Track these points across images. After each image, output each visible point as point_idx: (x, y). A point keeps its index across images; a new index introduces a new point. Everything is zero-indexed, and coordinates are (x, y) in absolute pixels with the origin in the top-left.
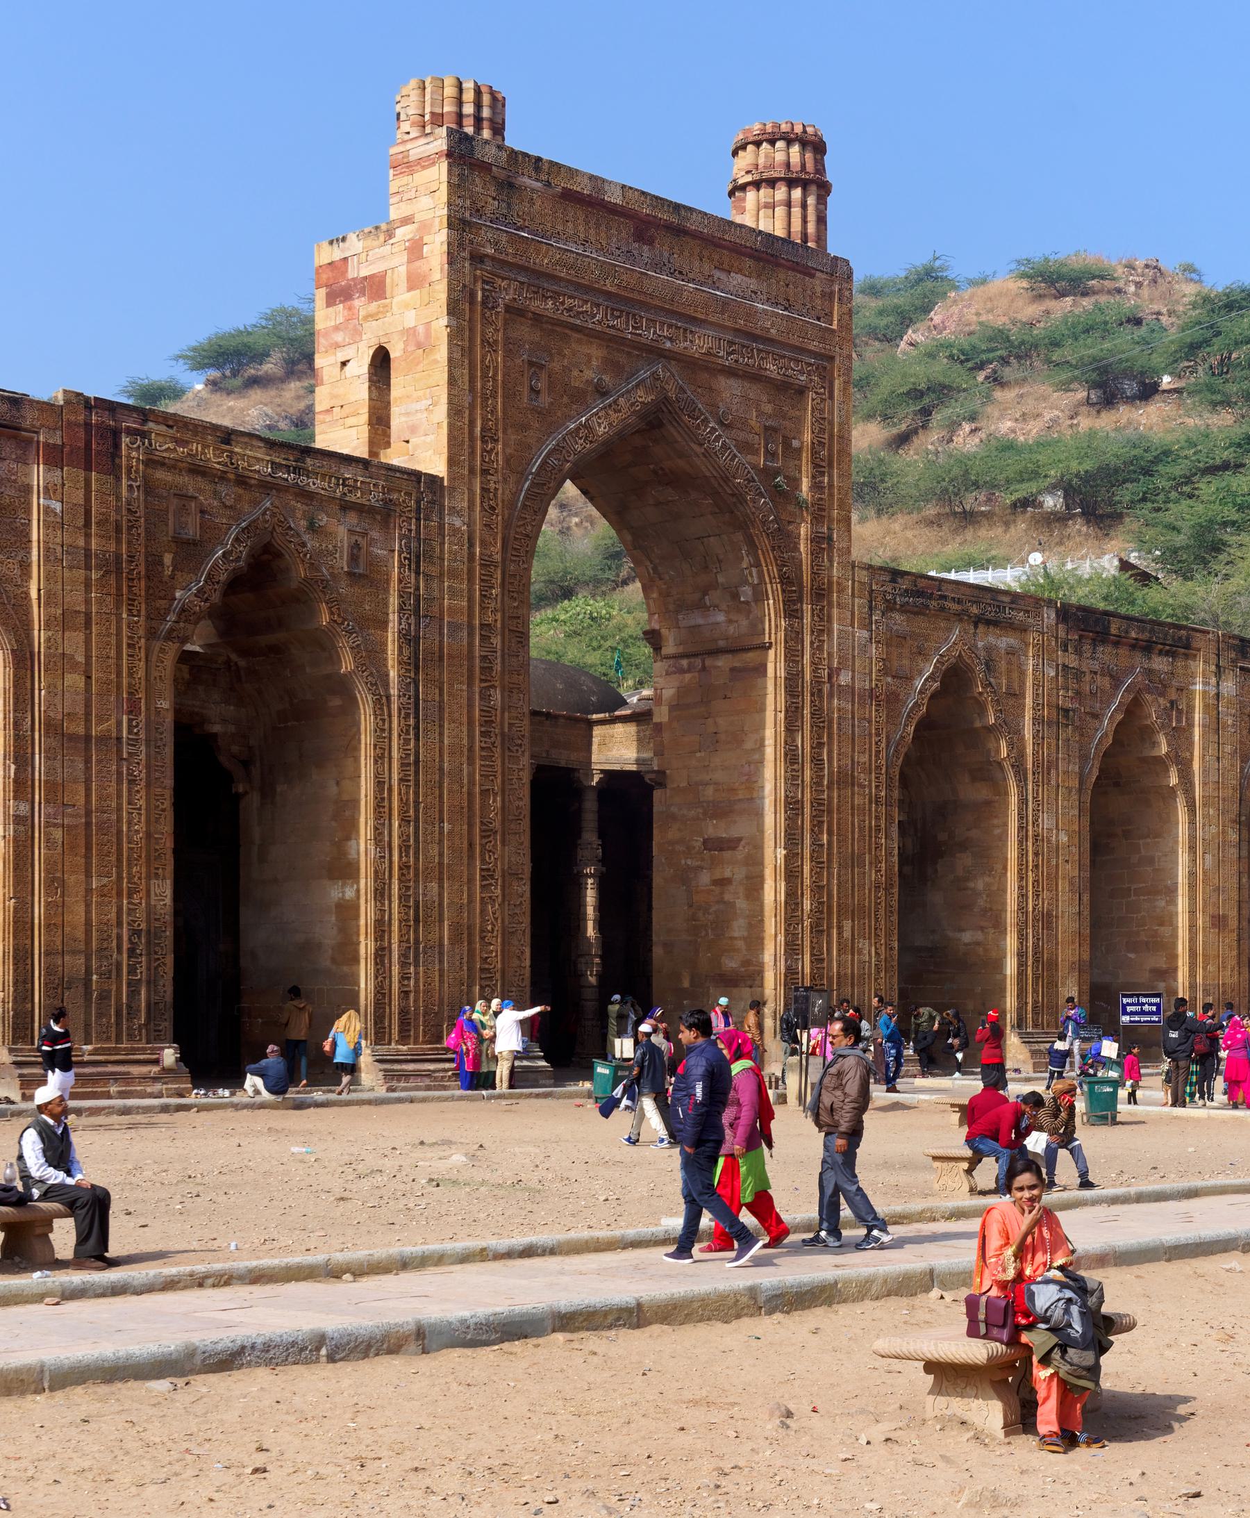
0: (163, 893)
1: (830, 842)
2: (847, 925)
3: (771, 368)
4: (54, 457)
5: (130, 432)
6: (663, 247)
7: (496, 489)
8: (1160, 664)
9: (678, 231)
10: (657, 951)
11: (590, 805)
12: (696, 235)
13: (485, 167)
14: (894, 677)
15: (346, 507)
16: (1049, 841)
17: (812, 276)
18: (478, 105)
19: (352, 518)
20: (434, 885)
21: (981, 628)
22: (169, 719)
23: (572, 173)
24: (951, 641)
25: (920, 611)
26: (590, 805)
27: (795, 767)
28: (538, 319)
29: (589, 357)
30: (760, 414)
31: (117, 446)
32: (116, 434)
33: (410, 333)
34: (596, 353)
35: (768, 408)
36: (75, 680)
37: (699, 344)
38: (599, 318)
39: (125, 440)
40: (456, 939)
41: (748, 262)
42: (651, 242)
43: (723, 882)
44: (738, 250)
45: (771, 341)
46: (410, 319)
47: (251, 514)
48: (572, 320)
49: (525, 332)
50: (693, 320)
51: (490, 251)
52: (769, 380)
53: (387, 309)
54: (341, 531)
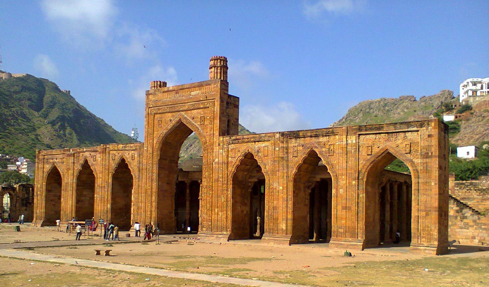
4: (100, 153)
13: (151, 94)
15: (132, 150)
16: (276, 189)
18: (157, 84)
21: (257, 143)
27: (206, 179)
28: (159, 113)
32: (106, 148)
34: (170, 114)
36: (101, 180)
37: (186, 108)
38: (168, 110)
41: (197, 88)
47: (120, 154)
51: (151, 106)
52: (202, 108)
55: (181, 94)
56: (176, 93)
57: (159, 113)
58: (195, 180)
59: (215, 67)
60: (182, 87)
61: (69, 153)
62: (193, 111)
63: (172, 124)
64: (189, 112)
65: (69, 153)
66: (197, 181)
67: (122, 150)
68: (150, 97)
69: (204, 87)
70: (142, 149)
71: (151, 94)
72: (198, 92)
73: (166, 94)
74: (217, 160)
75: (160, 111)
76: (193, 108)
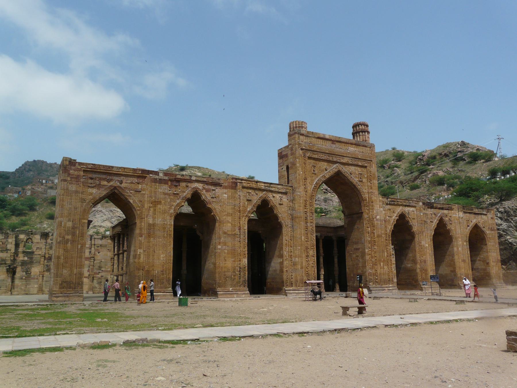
0: (245, 261)
2: (382, 264)
3: (360, 164)
4: (225, 187)
5: (239, 182)
6: (337, 145)
8: (446, 212)
9: (340, 142)
10: (347, 270)
11: (335, 243)
12: (343, 142)
13: (303, 135)
15: (279, 193)
19: (280, 195)
22: (246, 231)
23: (319, 134)
24: (399, 210)
25: (394, 205)
26: (335, 243)
28: (314, 159)
31: (237, 185)
32: (236, 183)
33: (291, 162)
34: (326, 164)
35: (360, 170)
36: (230, 225)
37: (345, 160)
38: (325, 157)
39: (238, 184)
40: (302, 268)
43: (357, 256)
45: (360, 159)
46: (291, 160)
49: (312, 161)
50: (344, 156)
51: (304, 148)
53: (288, 159)
54: (278, 196)
56: (333, 143)
57: (314, 159)
60: (339, 140)
61: (156, 177)
65: (156, 177)
67: (263, 190)
69: (361, 147)
71: (303, 135)
74: (378, 217)
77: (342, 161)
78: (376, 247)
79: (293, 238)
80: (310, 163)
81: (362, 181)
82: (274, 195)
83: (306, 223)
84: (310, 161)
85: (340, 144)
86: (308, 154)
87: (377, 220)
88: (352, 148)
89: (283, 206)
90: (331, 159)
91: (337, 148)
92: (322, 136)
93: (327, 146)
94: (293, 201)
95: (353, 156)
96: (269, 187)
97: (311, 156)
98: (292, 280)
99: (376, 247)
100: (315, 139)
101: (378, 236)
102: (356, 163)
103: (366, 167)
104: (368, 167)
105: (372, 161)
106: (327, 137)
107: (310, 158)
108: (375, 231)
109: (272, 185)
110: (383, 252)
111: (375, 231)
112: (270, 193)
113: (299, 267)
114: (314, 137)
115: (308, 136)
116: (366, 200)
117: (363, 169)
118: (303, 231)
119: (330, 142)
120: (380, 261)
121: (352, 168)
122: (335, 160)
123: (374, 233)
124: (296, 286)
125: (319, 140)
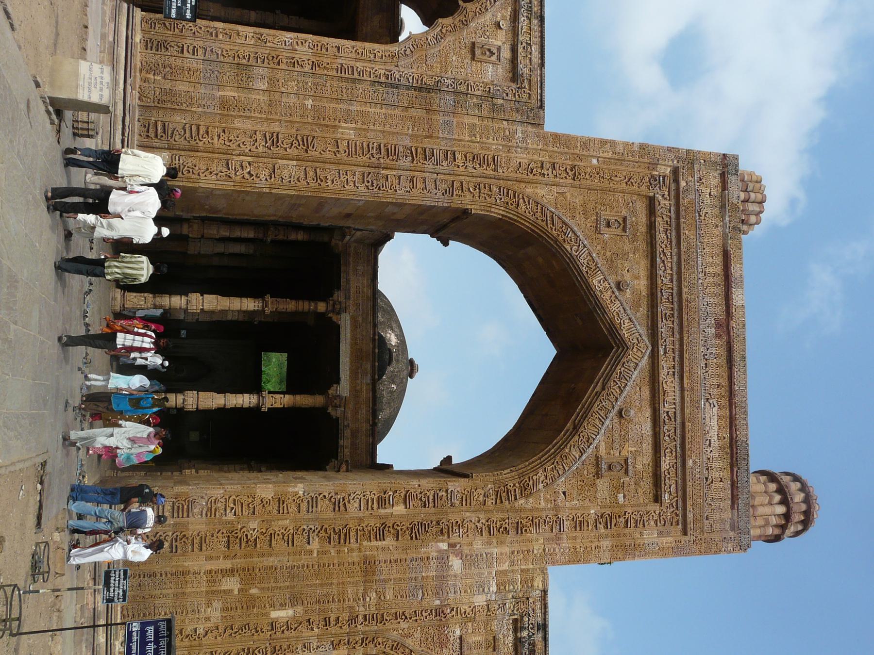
1: (311, 552)
3: (666, 463)
6: (717, 348)
7: (544, 175)
14: (461, 638)
15: (514, 50)
17: (732, 508)
19: (506, 54)
20: (265, 86)
27: (375, 506)
28: (651, 227)
29: (637, 278)
30: (635, 454)
34: (642, 284)
37: (669, 384)
38: (664, 279)
40: (224, 104)
42: (718, 336)
44: (732, 420)
48: (658, 255)
51: (683, 184)
54: (500, 40)
55: (714, 350)
56: (718, 325)
57: (651, 227)
58: (343, 280)
59: (787, 516)
60: (737, 357)
62: (648, 413)
63: (607, 296)
64: (646, 393)
66: (339, 288)
68: (713, 179)
69: (726, 474)
70: (519, 118)
72: (715, 443)
73: (719, 270)
74: (456, 563)
75: (661, 236)
76: (663, 416)
77: (665, 366)
78: (315, 545)
79: (349, 77)
80: (634, 213)
81: (598, 475)
82: (504, 24)
83: (412, 154)
84: (641, 207)
85: (723, 361)
86: (664, 203)
87: (443, 558)
88: (714, 422)
89: (468, 60)
90: (663, 308)
91: (704, 342)
92: (735, 270)
93: (706, 301)
94: (489, 96)
95: (688, 425)
96: (530, 10)
97: (659, 210)
98: (173, 51)
99: (315, 545)
100: (717, 241)
101: (368, 567)
102: (665, 441)
103: (657, 499)
104: (656, 507)
105: (685, 533)
106: (738, 298)
107: (651, 203)
108: (389, 541)
109: (535, 22)
110: (294, 600)
111: (389, 541)
112: (508, 13)
113: (229, 93)
114: (725, 237)
115: (723, 207)
116: (526, 490)
117: (647, 484)
118: (375, 138)
119: (719, 311)
120: (248, 575)
121: (641, 423)
122: (663, 328)
123: (380, 535)
124: (149, 68)
125: (719, 260)
